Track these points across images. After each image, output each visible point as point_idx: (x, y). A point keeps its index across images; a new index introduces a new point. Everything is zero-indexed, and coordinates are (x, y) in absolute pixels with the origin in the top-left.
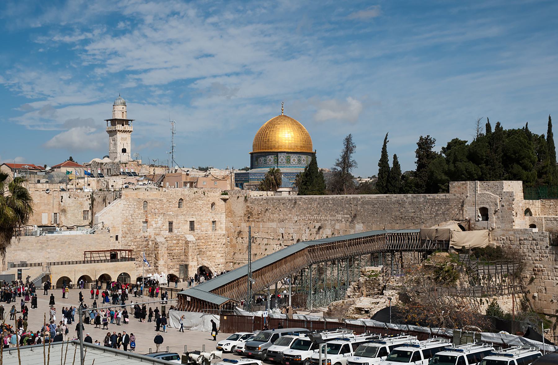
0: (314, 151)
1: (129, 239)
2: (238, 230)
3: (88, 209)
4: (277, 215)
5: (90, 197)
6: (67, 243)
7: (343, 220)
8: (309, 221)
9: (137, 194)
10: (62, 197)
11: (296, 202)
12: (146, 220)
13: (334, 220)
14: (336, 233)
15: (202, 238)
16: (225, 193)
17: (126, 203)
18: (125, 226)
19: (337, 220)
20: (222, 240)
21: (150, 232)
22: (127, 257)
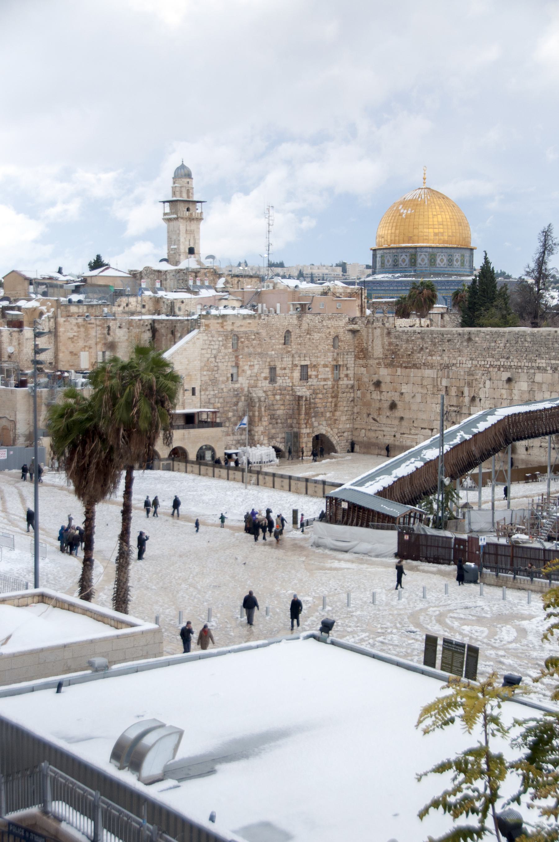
0: (472, 245)
1: (212, 393)
2: (375, 380)
4: (439, 358)
5: (149, 327)
7: (549, 368)
8: (491, 369)
10: (109, 327)
11: (469, 339)
13: (532, 367)
14: (536, 388)
15: (318, 391)
16: (353, 321)
17: (206, 338)
18: (205, 373)
19: (539, 368)
20: (348, 395)
21: (243, 382)
22: (209, 420)
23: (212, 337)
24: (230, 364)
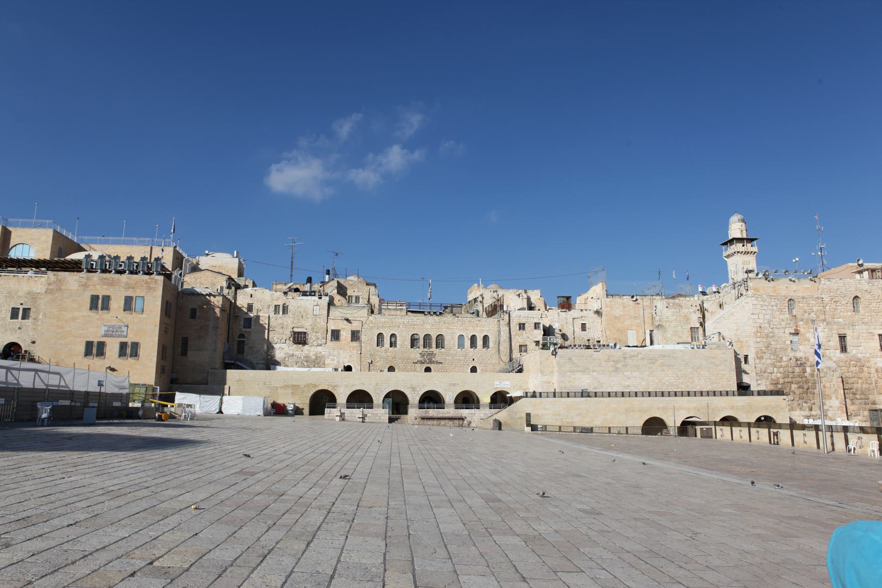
1: (769, 361)
3: (698, 325)
6: (658, 363)
9: (774, 287)
12: (796, 330)
17: (756, 302)
21: (805, 351)
23: (764, 301)
24: (787, 331)
